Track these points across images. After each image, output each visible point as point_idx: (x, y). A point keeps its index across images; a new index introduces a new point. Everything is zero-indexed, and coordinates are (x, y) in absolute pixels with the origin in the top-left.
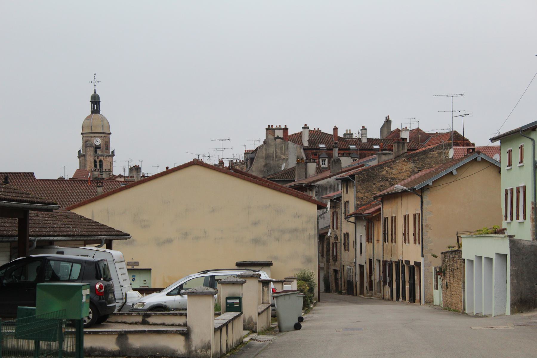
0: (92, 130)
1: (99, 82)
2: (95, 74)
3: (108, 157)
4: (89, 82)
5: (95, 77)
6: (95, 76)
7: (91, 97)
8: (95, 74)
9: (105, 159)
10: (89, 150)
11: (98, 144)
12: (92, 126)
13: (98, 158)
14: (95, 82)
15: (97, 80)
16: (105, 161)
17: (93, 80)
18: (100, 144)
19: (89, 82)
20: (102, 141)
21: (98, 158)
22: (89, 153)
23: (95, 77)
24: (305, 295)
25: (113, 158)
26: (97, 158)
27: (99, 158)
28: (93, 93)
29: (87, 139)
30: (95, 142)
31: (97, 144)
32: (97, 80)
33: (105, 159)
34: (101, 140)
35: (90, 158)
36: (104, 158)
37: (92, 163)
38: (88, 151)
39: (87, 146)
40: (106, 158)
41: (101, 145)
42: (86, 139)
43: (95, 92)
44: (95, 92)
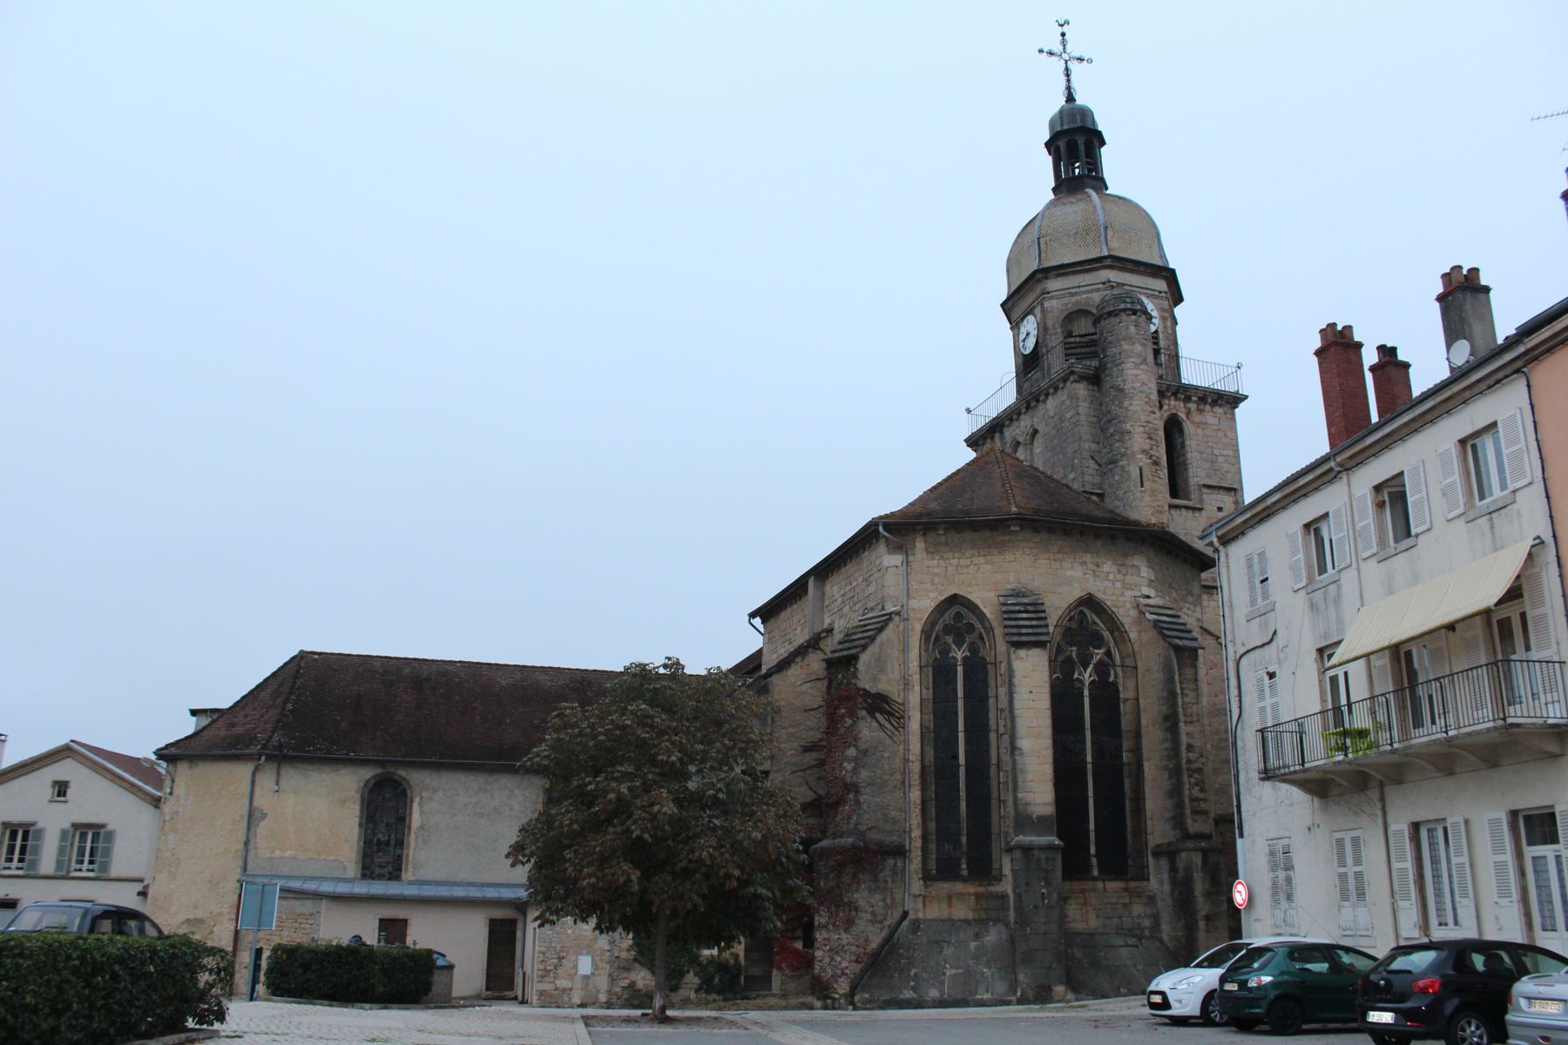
0: (1109, 250)
2: (1067, 22)
4: (1041, 51)
5: (1063, 35)
6: (1065, 29)
7: (1050, 121)
8: (1067, 22)
9: (1197, 418)
10: (1132, 329)
12: (1107, 228)
14: (1068, 60)
15: (1074, 49)
16: (1198, 425)
17: (1057, 48)
19: (1041, 51)
22: (1138, 348)
23: (1063, 35)
24: (960, 971)
25: (1233, 414)
27: (1165, 407)
28: (1060, 101)
29: (1073, 299)
32: (1074, 49)
35: (1144, 377)
36: (1193, 406)
37: (774, 656)
38: (1129, 338)
39: (1122, 306)
40: (1201, 411)
41: (1161, 336)
42: (1066, 300)
43: (1070, 98)
44: (1070, 98)
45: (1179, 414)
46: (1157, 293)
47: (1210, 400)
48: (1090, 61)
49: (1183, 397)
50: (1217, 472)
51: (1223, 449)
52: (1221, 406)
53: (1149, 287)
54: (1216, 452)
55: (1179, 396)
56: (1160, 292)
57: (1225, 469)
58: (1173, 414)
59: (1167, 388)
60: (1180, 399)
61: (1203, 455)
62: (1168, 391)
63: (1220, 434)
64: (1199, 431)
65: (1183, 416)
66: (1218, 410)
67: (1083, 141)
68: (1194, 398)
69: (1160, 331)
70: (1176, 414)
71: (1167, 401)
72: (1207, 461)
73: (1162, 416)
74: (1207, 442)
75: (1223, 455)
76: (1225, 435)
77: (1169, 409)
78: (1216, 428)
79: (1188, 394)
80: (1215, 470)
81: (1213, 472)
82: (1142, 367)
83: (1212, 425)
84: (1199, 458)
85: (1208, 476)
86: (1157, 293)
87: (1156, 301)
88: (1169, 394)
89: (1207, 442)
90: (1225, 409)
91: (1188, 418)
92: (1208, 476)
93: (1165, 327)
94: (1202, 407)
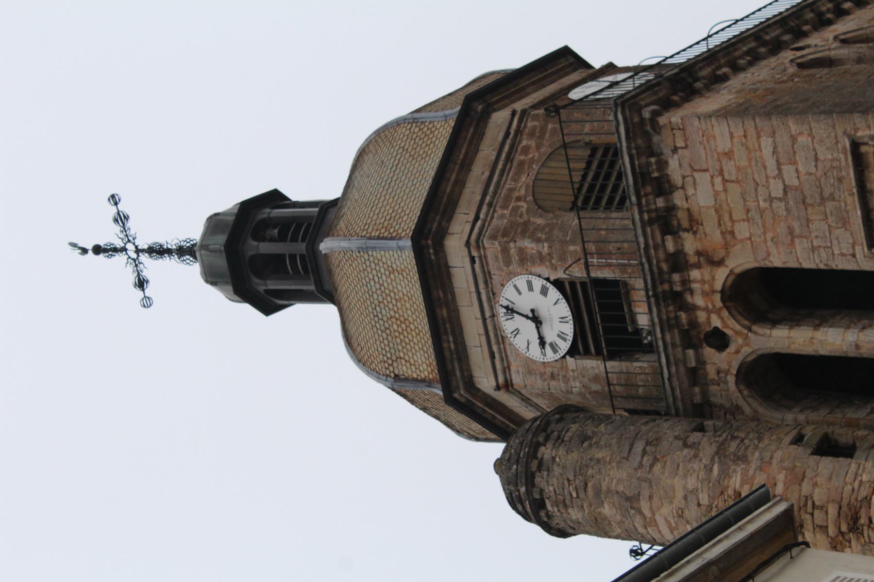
1: (89, 247)
3: (678, 199)
5: (97, 250)
9: (713, 235)
11: (564, 309)
13: (719, 340)
18: (554, 293)
20: (524, 259)
21: (719, 340)
23: (97, 250)
26: (708, 352)
27: (716, 322)
30: (550, 356)
31: (569, 329)
33: (713, 235)
34: (511, 275)
36: (690, 244)
40: (694, 224)
45: (718, 286)
46: (477, 266)
47: (660, 203)
48: (114, 200)
49: (676, 277)
50: (826, 194)
51: (765, 167)
52: (662, 165)
53: (473, 289)
54: (777, 190)
55: (677, 288)
56: (473, 260)
57: (813, 170)
58: (723, 300)
59: (671, 328)
60: (685, 282)
61: (797, 231)
62: (677, 318)
63: (729, 168)
64: (742, 230)
65: (721, 276)
66: (675, 169)
67: (255, 243)
68: (670, 246)
69: (560, 275)
70: (722, 292)
71: (702, 316)
72: (808, 221)
73: (737, 333)
74: (762, 212)
75: (779, 164)
76: (729, 155)
77: (718, 312)
78: (718, 180)
79: (665, 267)
80: (823, 199)
81: (830, 205)
82: (647, 513)
83: (716, 194)
84: (806, 244)
85: (845, 223)
86: (477, 266)
87: (496, 279)
88: (683, 316)
89: (762, 212)
90: (667, 151)
91: (720, 263)
92: (845, 223)
93: (541, 258)
94: (682, 215)
